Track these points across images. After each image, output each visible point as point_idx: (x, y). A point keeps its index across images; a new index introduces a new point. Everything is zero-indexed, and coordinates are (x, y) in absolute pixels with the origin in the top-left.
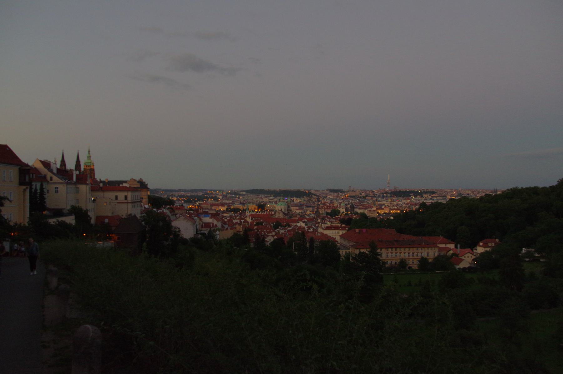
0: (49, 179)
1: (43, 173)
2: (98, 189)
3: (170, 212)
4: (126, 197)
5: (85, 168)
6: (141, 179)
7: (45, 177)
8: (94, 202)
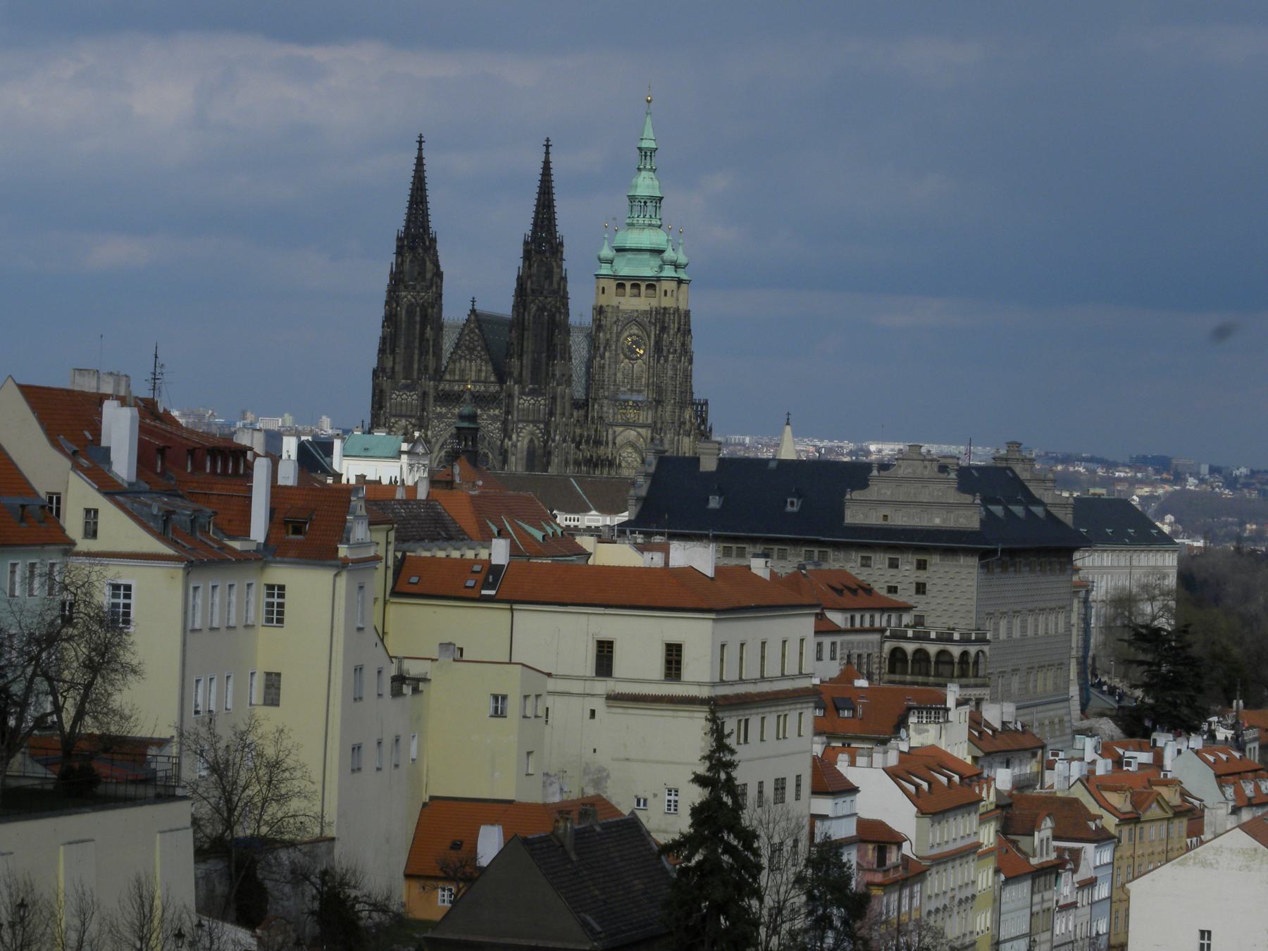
0: (73, 523)
1: (42, 485)
2: (470, 583)
3: (1223, 777)
4: (674, 655)
5: (611, 299)
6: (1014, 445)
7: (53, 506)
8: (407, 689)
